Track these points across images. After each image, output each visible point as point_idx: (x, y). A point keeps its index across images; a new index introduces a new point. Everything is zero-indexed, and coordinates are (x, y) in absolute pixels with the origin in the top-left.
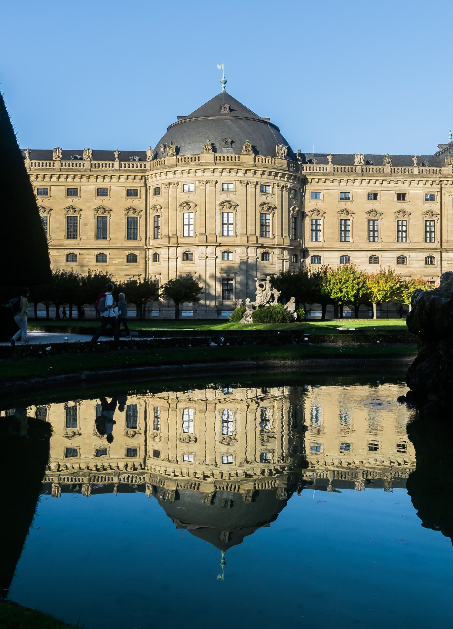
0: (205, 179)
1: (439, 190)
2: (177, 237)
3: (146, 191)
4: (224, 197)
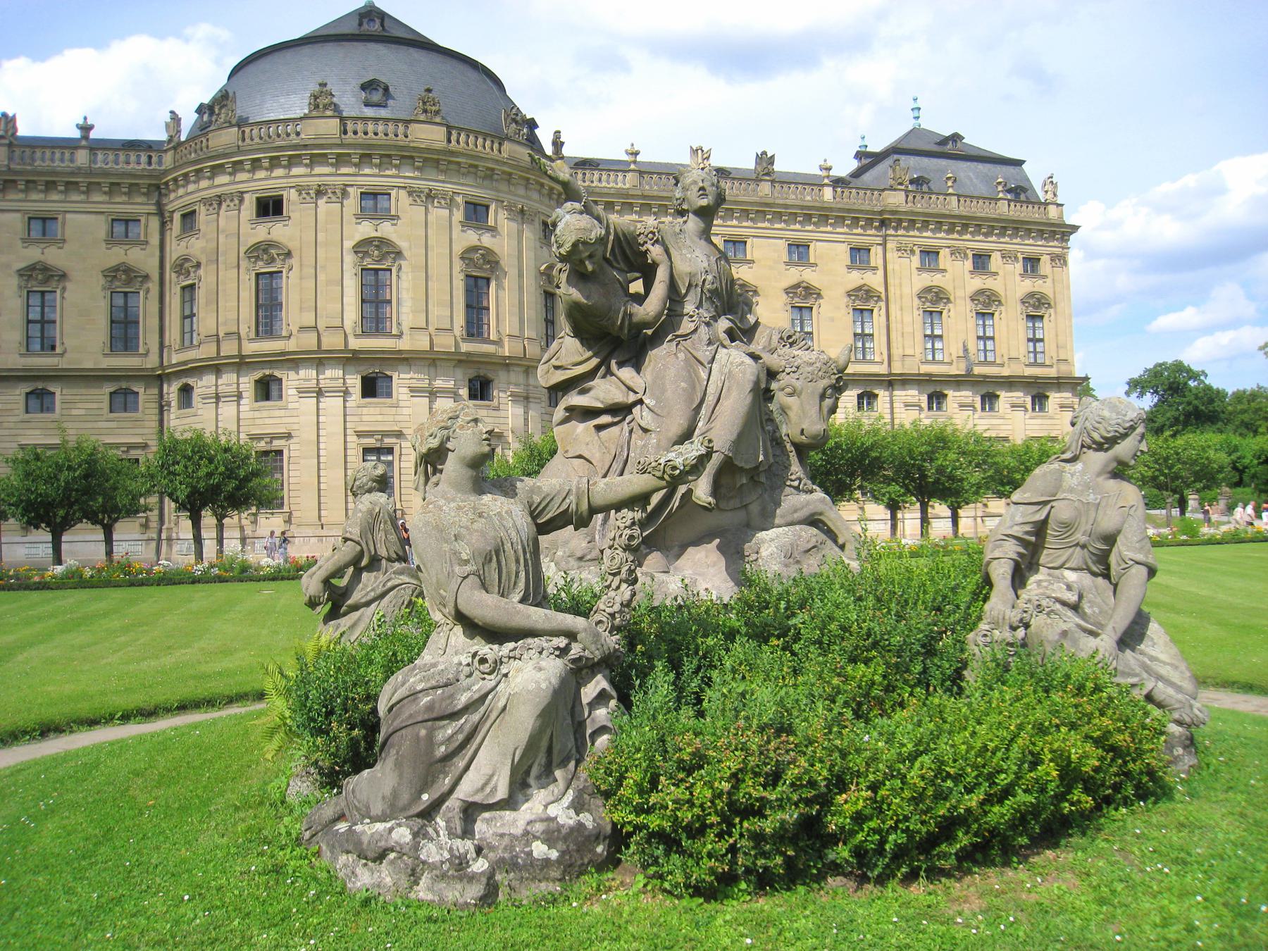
0: (314, 181)
1: (879, 240)
2: (240, 339)
3: (163, 225)
4: (366, 230)
